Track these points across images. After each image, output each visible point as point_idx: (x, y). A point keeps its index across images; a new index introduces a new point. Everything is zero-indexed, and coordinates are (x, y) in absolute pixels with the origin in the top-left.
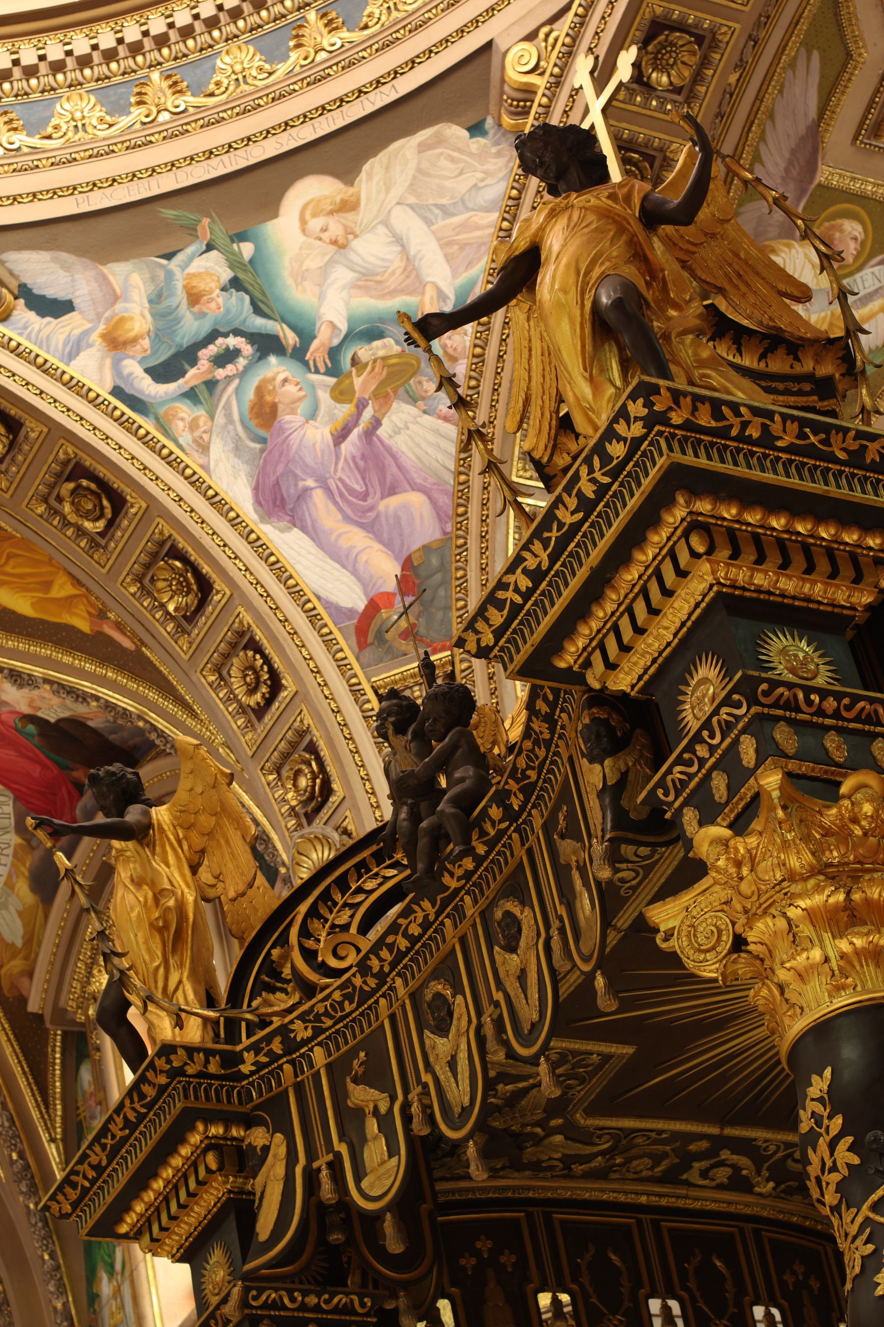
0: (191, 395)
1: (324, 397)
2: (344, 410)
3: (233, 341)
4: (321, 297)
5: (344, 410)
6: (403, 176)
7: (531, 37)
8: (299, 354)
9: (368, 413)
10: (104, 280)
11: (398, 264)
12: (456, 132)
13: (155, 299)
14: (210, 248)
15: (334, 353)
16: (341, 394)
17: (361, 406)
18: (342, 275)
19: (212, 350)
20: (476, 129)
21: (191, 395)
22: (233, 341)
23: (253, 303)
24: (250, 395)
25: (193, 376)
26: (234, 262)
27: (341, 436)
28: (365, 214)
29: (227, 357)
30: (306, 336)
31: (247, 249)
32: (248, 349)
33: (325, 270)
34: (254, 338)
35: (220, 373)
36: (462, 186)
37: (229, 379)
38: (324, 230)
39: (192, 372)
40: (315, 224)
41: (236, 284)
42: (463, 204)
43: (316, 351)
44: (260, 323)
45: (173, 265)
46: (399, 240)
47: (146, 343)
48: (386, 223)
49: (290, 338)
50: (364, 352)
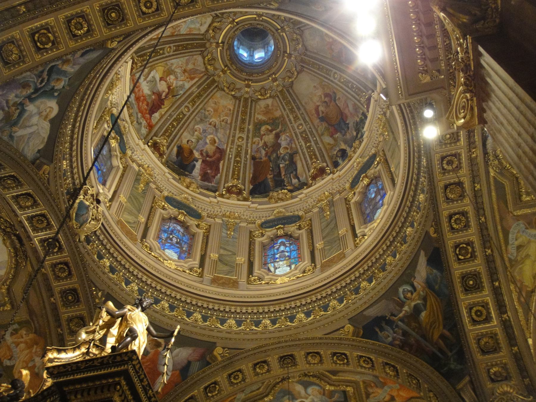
1: (17, 100)
2: (11, 103)
4: (35, 106)
5: (11, 103)
9: (7, 109)
10: (79, 64)
11: (28, 124)
12: (41, 147)
14: (63, 87)
17: (9, 107)
19: (46, 79)
20: (39, 151)
23: (46, 91)
24: (31, 84)
26: (56, 91)
27: (7, 102)
31: (56, 94)
37: (38, 80)
38: (46, 111)
39: (46, 73)
40: (48, 110)
41: (53, 89)
42: (28, 142)
45: (67, 79)
47: (60, 67)
48: (36, 125)
49: (33, 96)
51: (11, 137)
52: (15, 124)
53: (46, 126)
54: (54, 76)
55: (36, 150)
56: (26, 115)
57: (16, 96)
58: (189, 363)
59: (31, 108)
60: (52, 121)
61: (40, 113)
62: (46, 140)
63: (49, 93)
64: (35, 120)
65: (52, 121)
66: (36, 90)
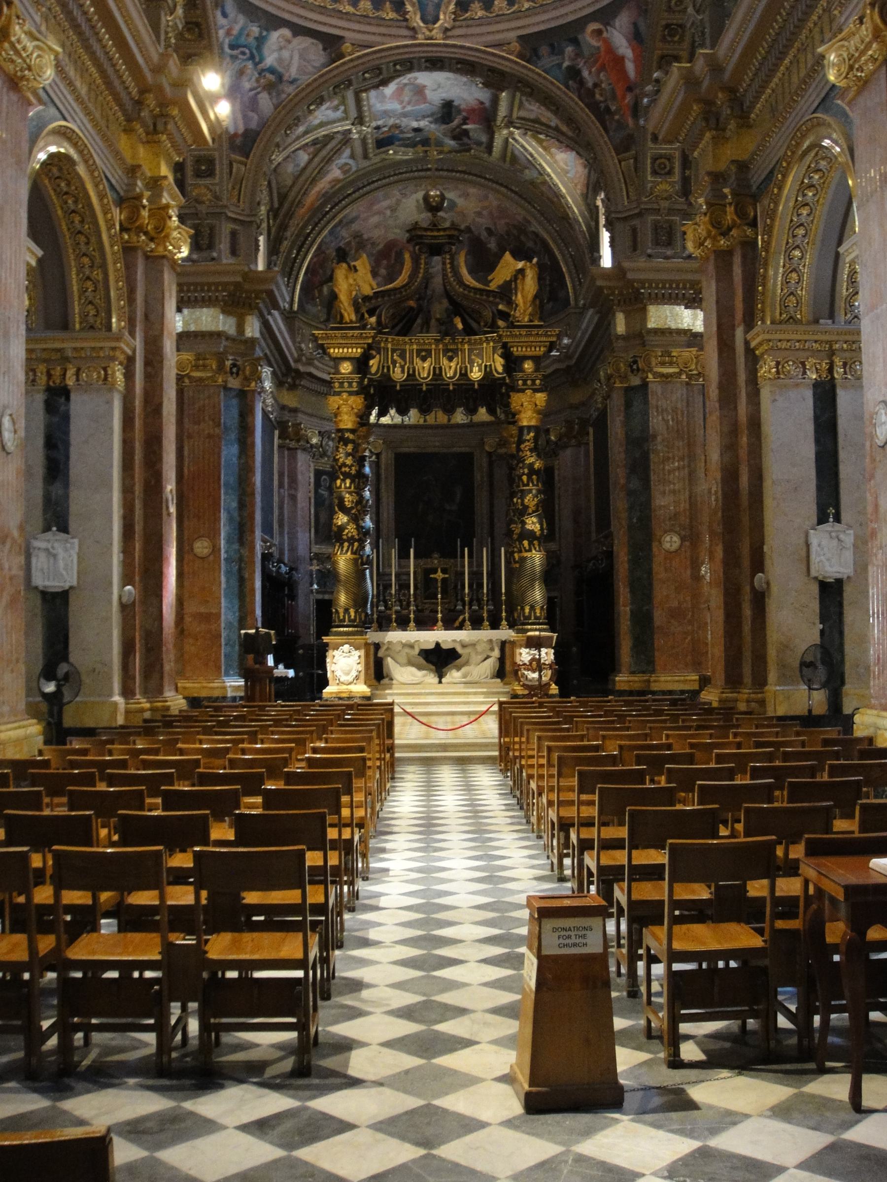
0: (232, 56)
1: (254, 79)
2: (255, 85)
3: (247, 51)
5: (255, 85)
6: (304, 45)
7: (353, 44)
8: (256, 64)
12: (321, 47)
13: (242, 29)
15: (263, 70)
16: (257, 81)
18: (275, 55)
20: (325, 49)
21: (232, 56)
22: (247, 51)
25: (235, 52)
27: (251, 90)
28: (290, 46)
29: (243, 53)
30: (260, 62)
31: (265, 33)
32: (248, 55)
33: (274, 51)
34: (251, 53)
35: (241, 56)
36: (313, 57)
41: (257, 39)
43: (261, 66)
44: (254, 51)
46: (291, 57)
49: (257, 60)
50: (268, 75)
51: (292, 82)
52: (280, 77)
53: (300, 39)
54: (242, 40)
55: (322, 52)
56: (275, 64)
57: (249, 80)
58: (635, 25)
59: (270, 60)
60: (295, 34)
61: (281, 49)
62: (315, 41)
63: (261, 40)
64: (286, 54)
65: (295, 34)
66: (252, 57)
